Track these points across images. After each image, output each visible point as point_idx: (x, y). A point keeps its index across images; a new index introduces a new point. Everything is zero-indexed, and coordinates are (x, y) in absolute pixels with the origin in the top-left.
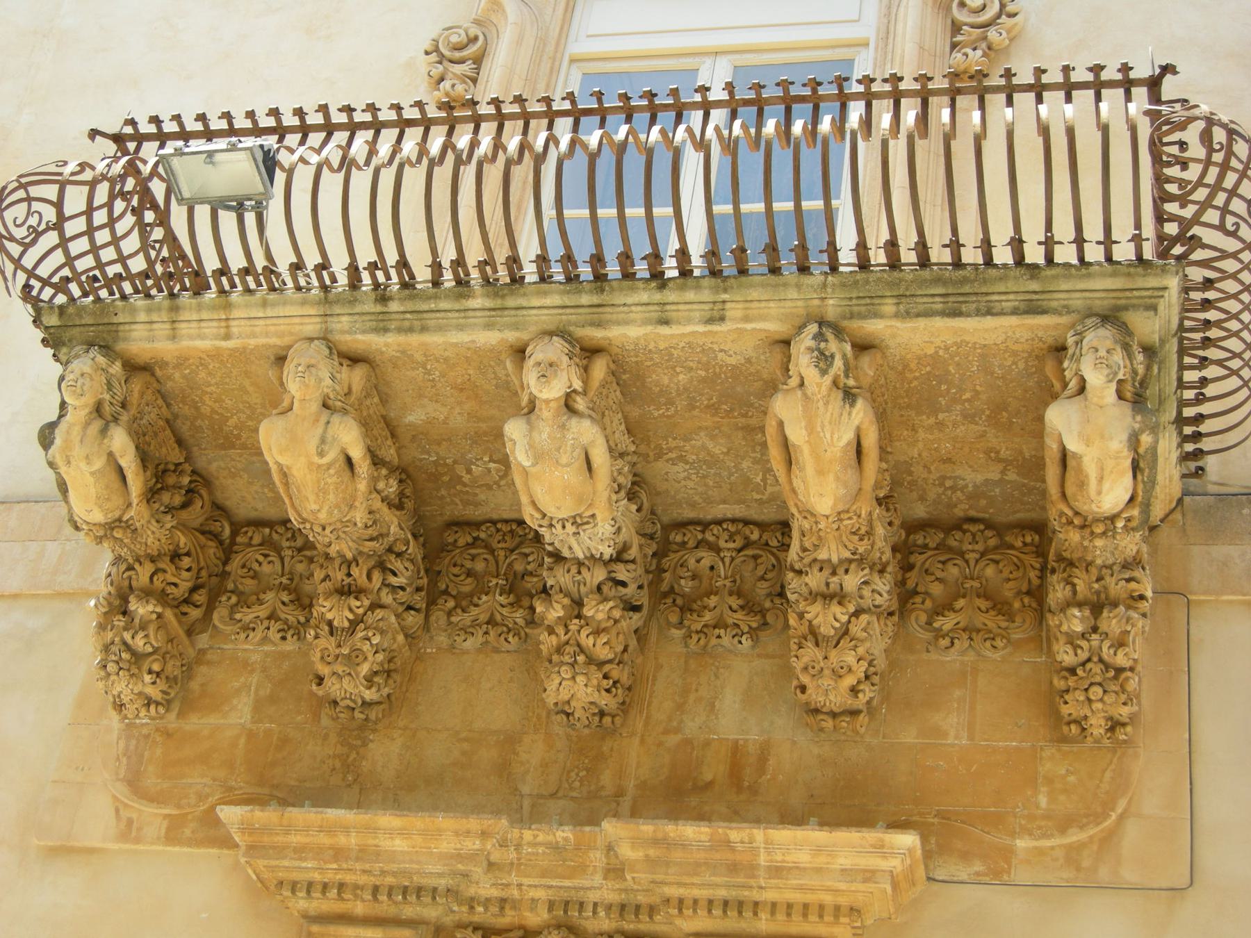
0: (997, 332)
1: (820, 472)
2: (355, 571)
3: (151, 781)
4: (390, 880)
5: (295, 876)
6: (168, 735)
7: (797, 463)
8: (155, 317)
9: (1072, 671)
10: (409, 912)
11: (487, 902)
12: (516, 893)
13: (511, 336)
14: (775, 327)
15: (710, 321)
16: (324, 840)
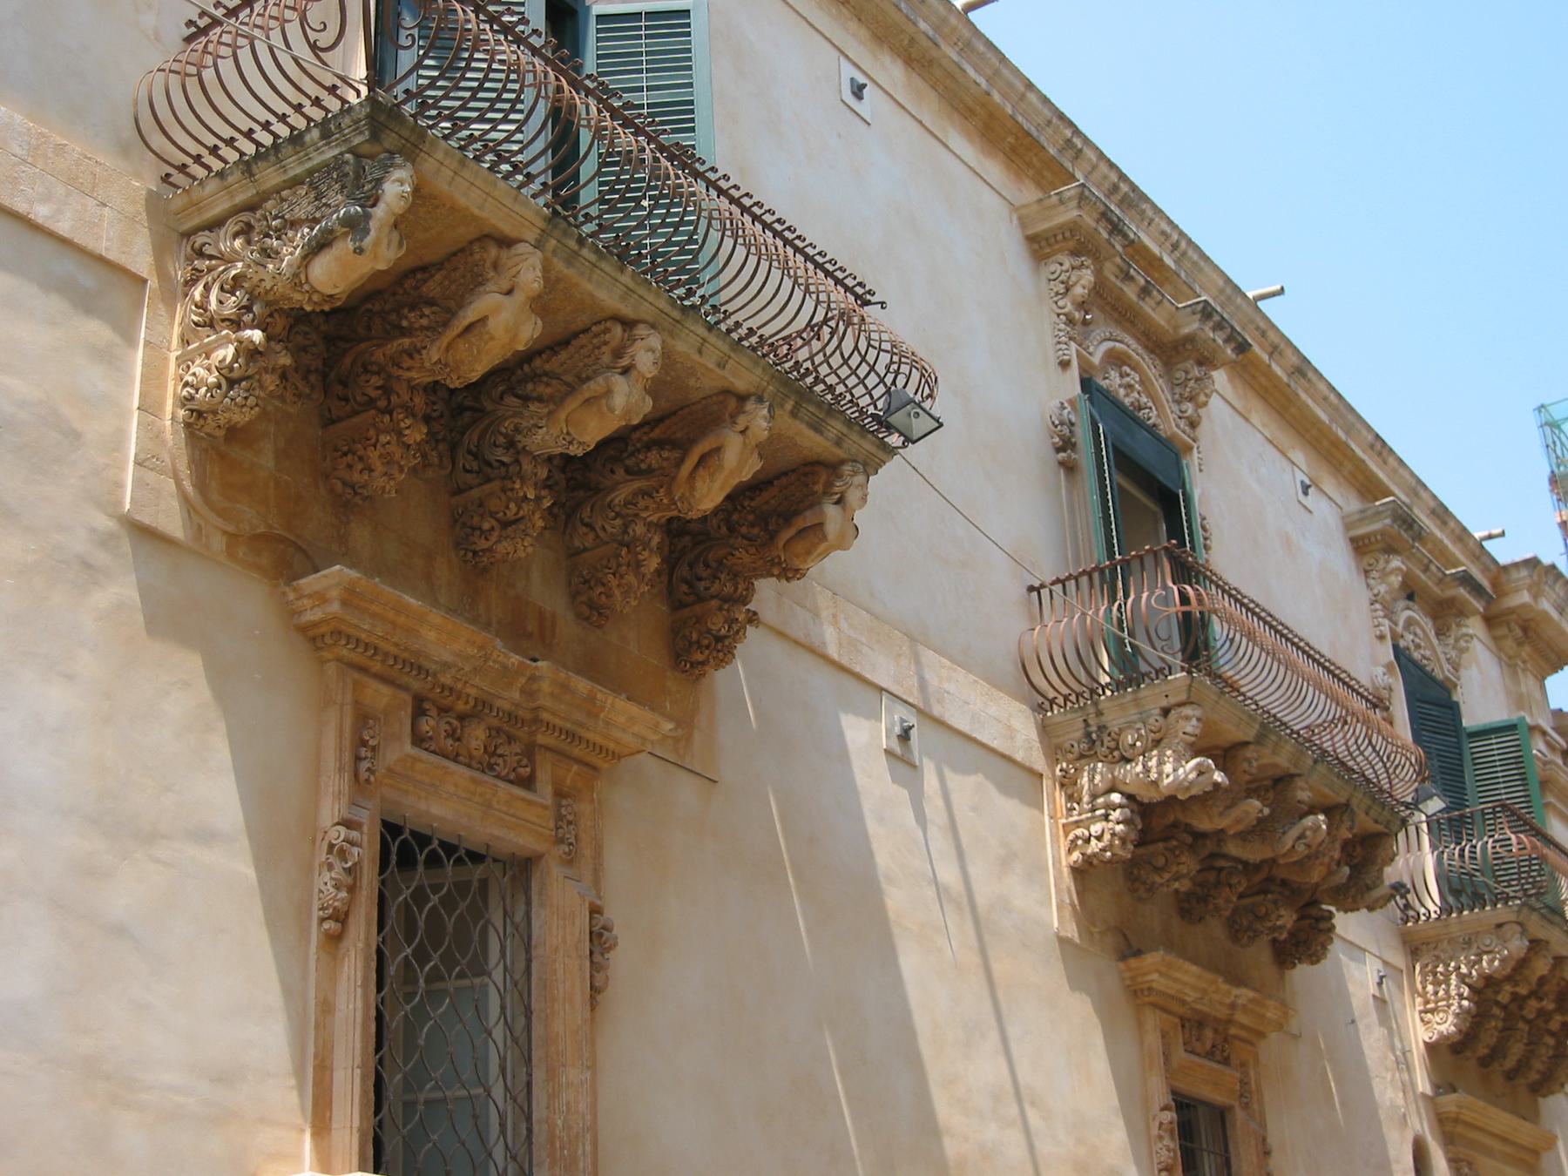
0: (814, 443)
1: (721, 489)
2: (417, 400)
3: (215, 496)
4: (406, 655)
5: (351, 631)
6: (222, 456)
7: (712, 475)
8: (447, 162)
9: (719, 639)
10: (405, 679)
11: (443, 687)
12: (459, 686)
13: (627, 311)
14: (741, 385)
15: (719, 365)
16: (391, 615)
